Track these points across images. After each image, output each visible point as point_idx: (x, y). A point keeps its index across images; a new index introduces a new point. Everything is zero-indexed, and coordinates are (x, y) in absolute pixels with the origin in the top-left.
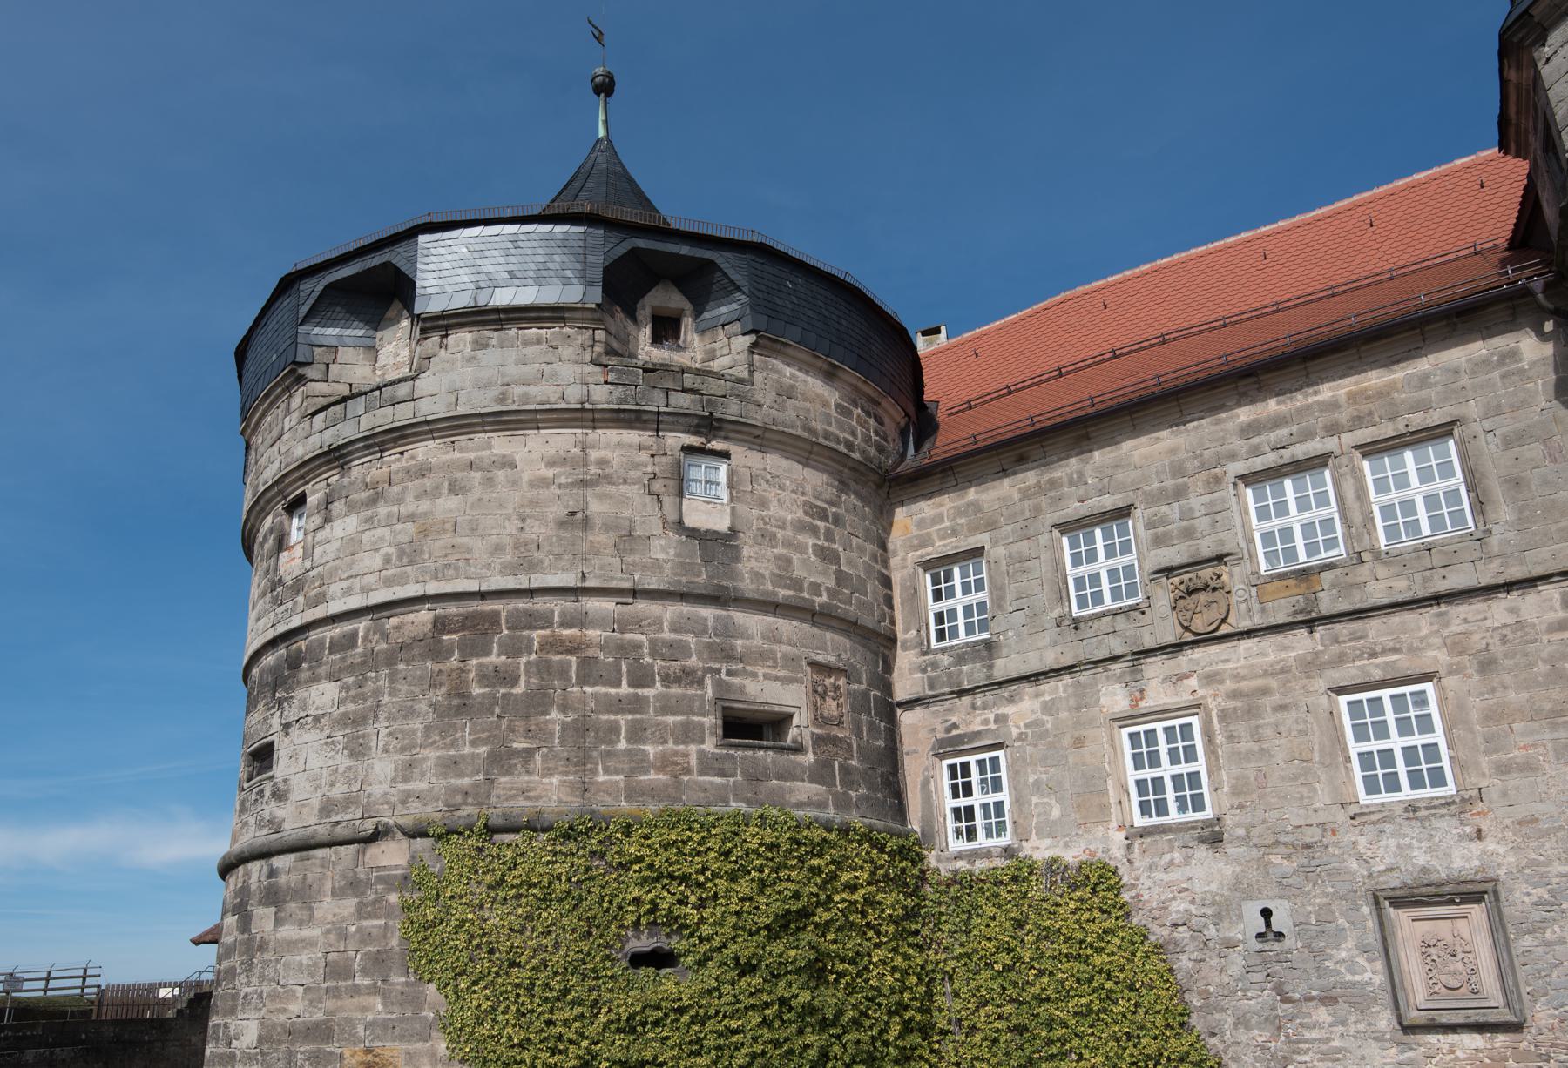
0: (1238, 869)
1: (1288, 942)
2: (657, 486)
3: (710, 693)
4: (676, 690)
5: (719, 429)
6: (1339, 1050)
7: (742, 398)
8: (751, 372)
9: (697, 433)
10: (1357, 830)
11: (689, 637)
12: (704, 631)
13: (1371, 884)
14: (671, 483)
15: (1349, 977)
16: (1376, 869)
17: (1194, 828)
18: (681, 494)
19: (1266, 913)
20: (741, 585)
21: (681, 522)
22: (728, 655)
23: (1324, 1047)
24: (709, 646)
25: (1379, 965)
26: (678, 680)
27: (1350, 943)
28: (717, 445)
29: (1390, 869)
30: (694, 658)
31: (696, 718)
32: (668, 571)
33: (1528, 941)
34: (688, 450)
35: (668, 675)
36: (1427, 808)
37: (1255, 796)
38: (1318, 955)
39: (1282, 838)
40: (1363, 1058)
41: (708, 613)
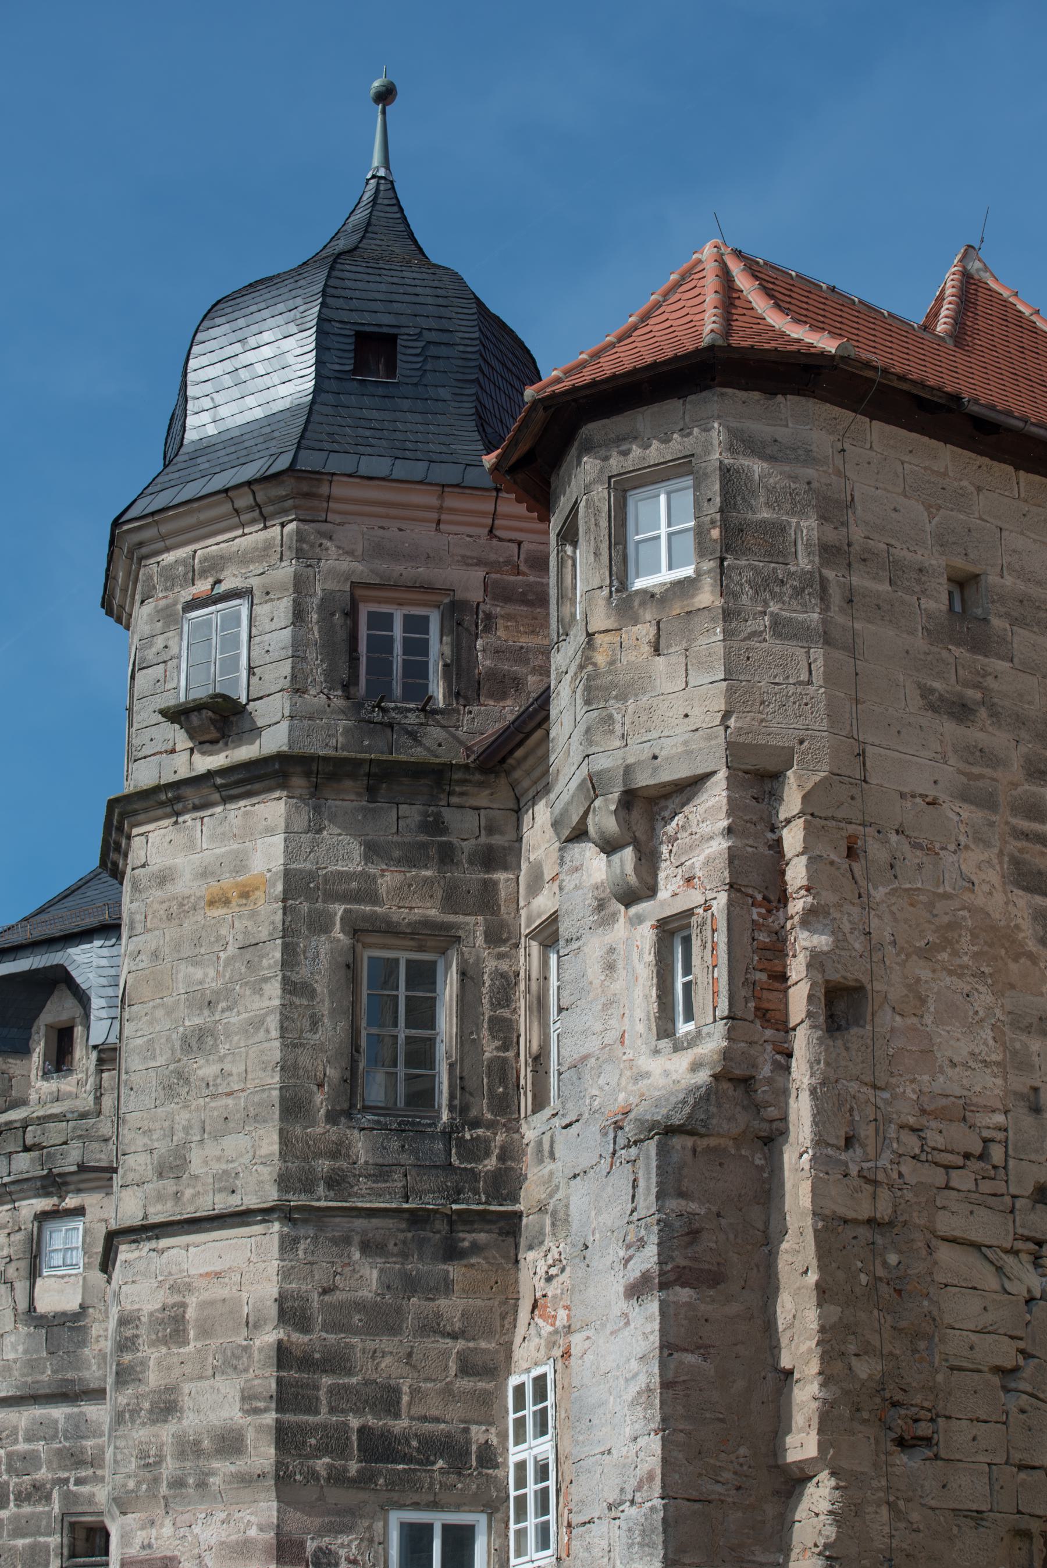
2: (11, 1273)
3: (56, 1508)
4: (27, 1509)
5: (66, 1184)
7: (85, 1137)
8: (98, 1099)
9: (48, 1195)
11: (40, 1446)
12: (55, 1436)
14: (24, 1265)
18: (34, 1273)
20: (86, 1374)
21: (31, 1308)
22: (75, 1459)
24: (59, 1452)
26: (28, 1498)
28: (71, 1202)
30: (44, 1470)
31: (42, 1539)
32: (16, 1373)
34: (43, 1217)
35: (20, 1493)
41: (58, 1413)
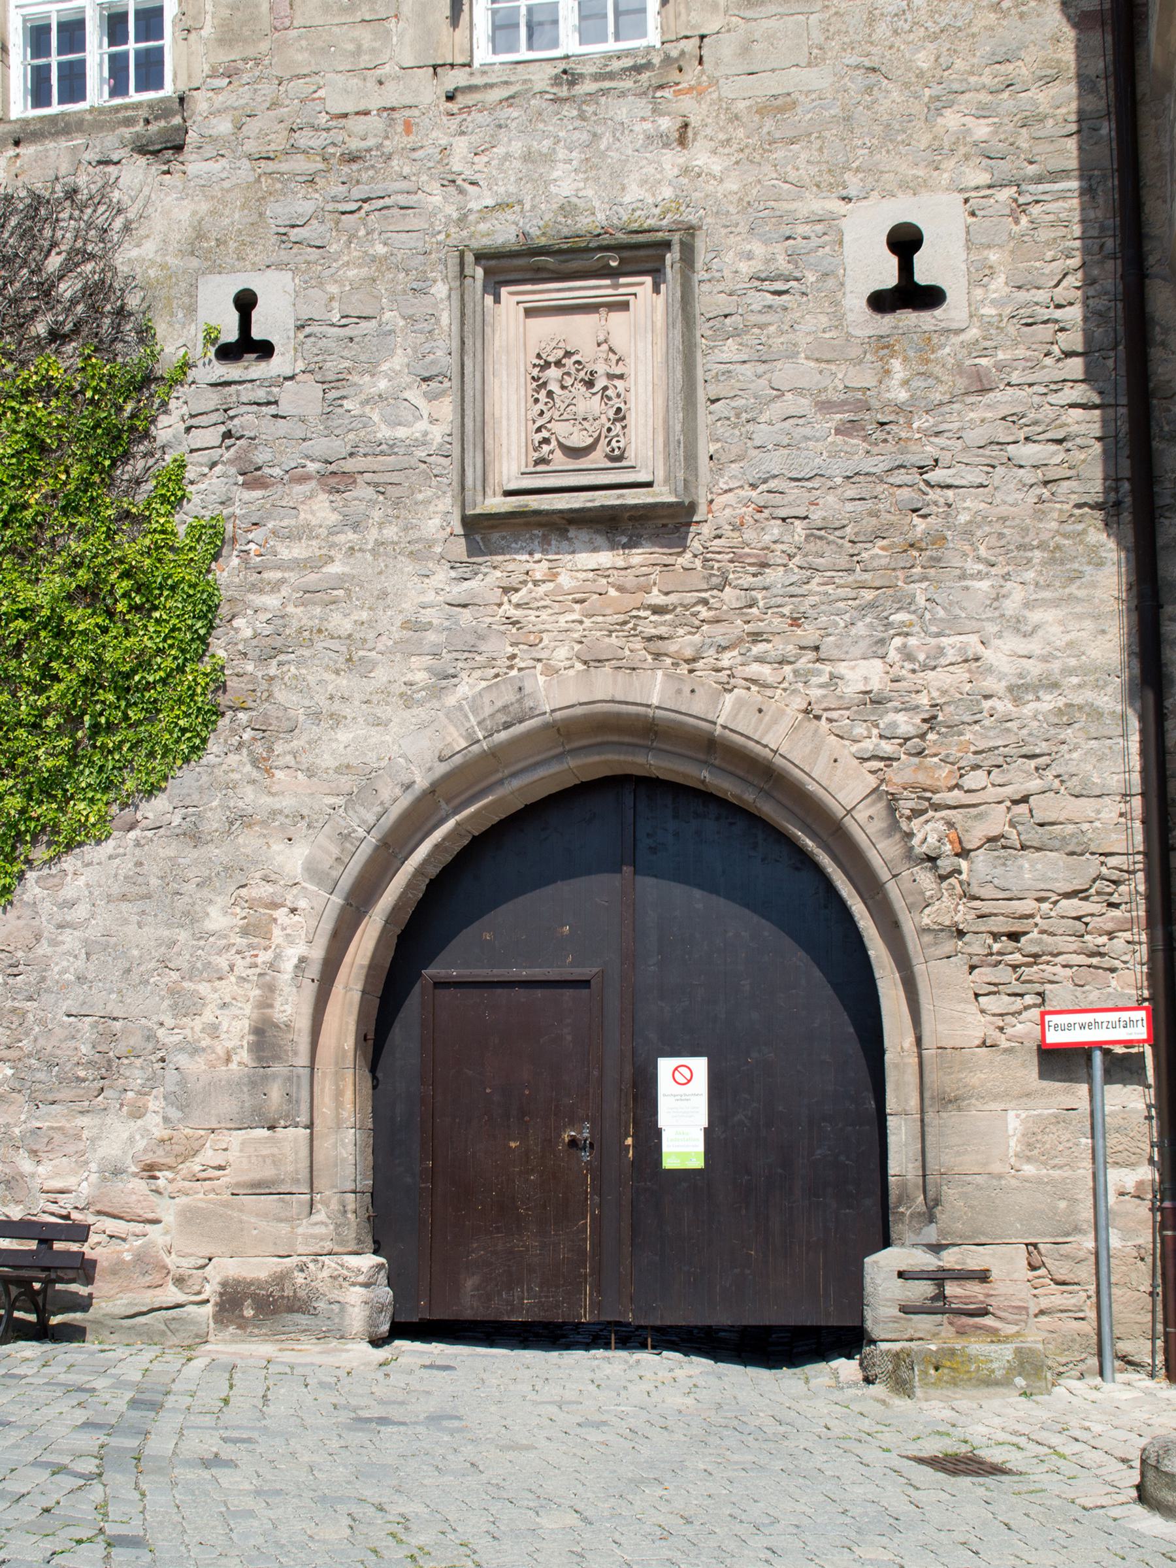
0: (204, 207)
1: (277, 365)
6: (340, 581)
10: (453, 124)
13: (458, 236)
15: (384, 432)
16: (474, 205)
17: (129, 122)
19: (245, 303)
23: (312, 578)
25: (446, 408)
27: (398, 361)
29: (501, 206)
33: (730, 350)
36: (597, 77)
37: (264, 46)
38: (334, 386)
39: (304, 139)
40: (384, 594)
